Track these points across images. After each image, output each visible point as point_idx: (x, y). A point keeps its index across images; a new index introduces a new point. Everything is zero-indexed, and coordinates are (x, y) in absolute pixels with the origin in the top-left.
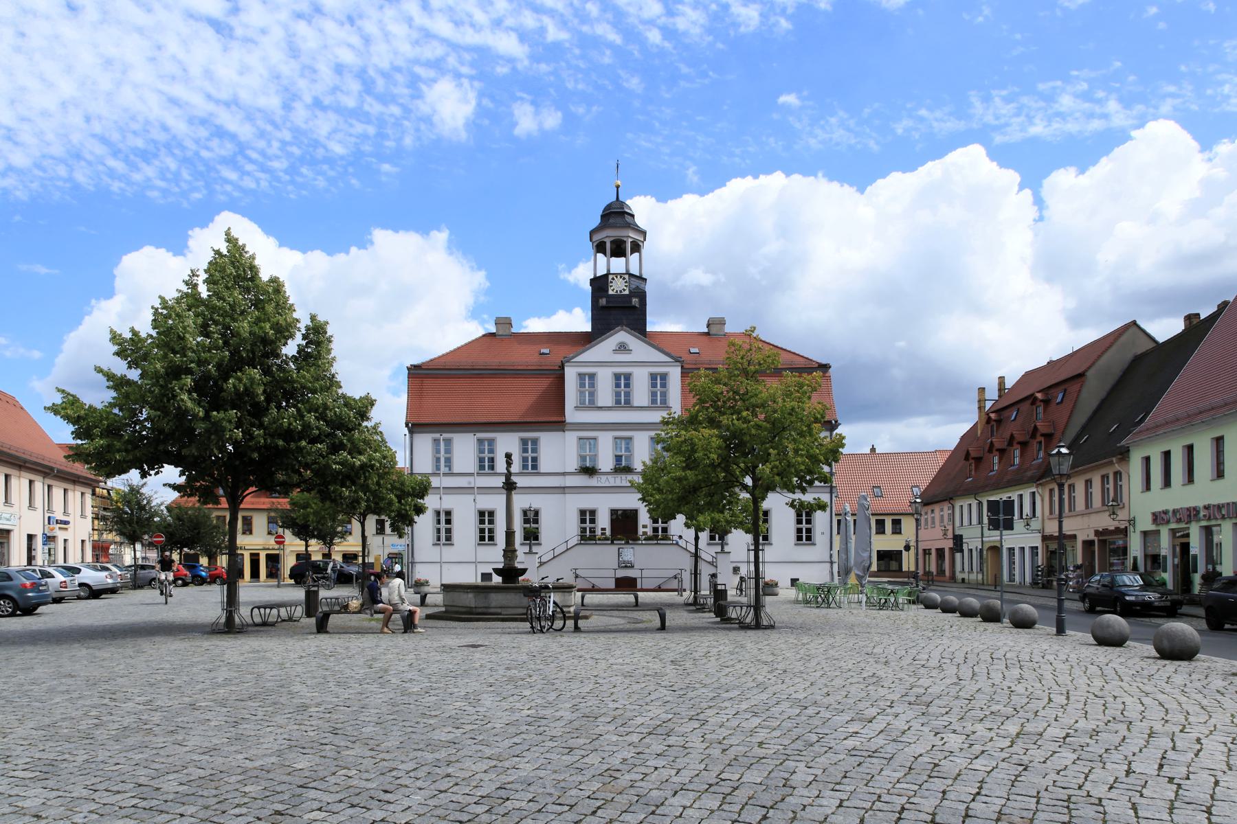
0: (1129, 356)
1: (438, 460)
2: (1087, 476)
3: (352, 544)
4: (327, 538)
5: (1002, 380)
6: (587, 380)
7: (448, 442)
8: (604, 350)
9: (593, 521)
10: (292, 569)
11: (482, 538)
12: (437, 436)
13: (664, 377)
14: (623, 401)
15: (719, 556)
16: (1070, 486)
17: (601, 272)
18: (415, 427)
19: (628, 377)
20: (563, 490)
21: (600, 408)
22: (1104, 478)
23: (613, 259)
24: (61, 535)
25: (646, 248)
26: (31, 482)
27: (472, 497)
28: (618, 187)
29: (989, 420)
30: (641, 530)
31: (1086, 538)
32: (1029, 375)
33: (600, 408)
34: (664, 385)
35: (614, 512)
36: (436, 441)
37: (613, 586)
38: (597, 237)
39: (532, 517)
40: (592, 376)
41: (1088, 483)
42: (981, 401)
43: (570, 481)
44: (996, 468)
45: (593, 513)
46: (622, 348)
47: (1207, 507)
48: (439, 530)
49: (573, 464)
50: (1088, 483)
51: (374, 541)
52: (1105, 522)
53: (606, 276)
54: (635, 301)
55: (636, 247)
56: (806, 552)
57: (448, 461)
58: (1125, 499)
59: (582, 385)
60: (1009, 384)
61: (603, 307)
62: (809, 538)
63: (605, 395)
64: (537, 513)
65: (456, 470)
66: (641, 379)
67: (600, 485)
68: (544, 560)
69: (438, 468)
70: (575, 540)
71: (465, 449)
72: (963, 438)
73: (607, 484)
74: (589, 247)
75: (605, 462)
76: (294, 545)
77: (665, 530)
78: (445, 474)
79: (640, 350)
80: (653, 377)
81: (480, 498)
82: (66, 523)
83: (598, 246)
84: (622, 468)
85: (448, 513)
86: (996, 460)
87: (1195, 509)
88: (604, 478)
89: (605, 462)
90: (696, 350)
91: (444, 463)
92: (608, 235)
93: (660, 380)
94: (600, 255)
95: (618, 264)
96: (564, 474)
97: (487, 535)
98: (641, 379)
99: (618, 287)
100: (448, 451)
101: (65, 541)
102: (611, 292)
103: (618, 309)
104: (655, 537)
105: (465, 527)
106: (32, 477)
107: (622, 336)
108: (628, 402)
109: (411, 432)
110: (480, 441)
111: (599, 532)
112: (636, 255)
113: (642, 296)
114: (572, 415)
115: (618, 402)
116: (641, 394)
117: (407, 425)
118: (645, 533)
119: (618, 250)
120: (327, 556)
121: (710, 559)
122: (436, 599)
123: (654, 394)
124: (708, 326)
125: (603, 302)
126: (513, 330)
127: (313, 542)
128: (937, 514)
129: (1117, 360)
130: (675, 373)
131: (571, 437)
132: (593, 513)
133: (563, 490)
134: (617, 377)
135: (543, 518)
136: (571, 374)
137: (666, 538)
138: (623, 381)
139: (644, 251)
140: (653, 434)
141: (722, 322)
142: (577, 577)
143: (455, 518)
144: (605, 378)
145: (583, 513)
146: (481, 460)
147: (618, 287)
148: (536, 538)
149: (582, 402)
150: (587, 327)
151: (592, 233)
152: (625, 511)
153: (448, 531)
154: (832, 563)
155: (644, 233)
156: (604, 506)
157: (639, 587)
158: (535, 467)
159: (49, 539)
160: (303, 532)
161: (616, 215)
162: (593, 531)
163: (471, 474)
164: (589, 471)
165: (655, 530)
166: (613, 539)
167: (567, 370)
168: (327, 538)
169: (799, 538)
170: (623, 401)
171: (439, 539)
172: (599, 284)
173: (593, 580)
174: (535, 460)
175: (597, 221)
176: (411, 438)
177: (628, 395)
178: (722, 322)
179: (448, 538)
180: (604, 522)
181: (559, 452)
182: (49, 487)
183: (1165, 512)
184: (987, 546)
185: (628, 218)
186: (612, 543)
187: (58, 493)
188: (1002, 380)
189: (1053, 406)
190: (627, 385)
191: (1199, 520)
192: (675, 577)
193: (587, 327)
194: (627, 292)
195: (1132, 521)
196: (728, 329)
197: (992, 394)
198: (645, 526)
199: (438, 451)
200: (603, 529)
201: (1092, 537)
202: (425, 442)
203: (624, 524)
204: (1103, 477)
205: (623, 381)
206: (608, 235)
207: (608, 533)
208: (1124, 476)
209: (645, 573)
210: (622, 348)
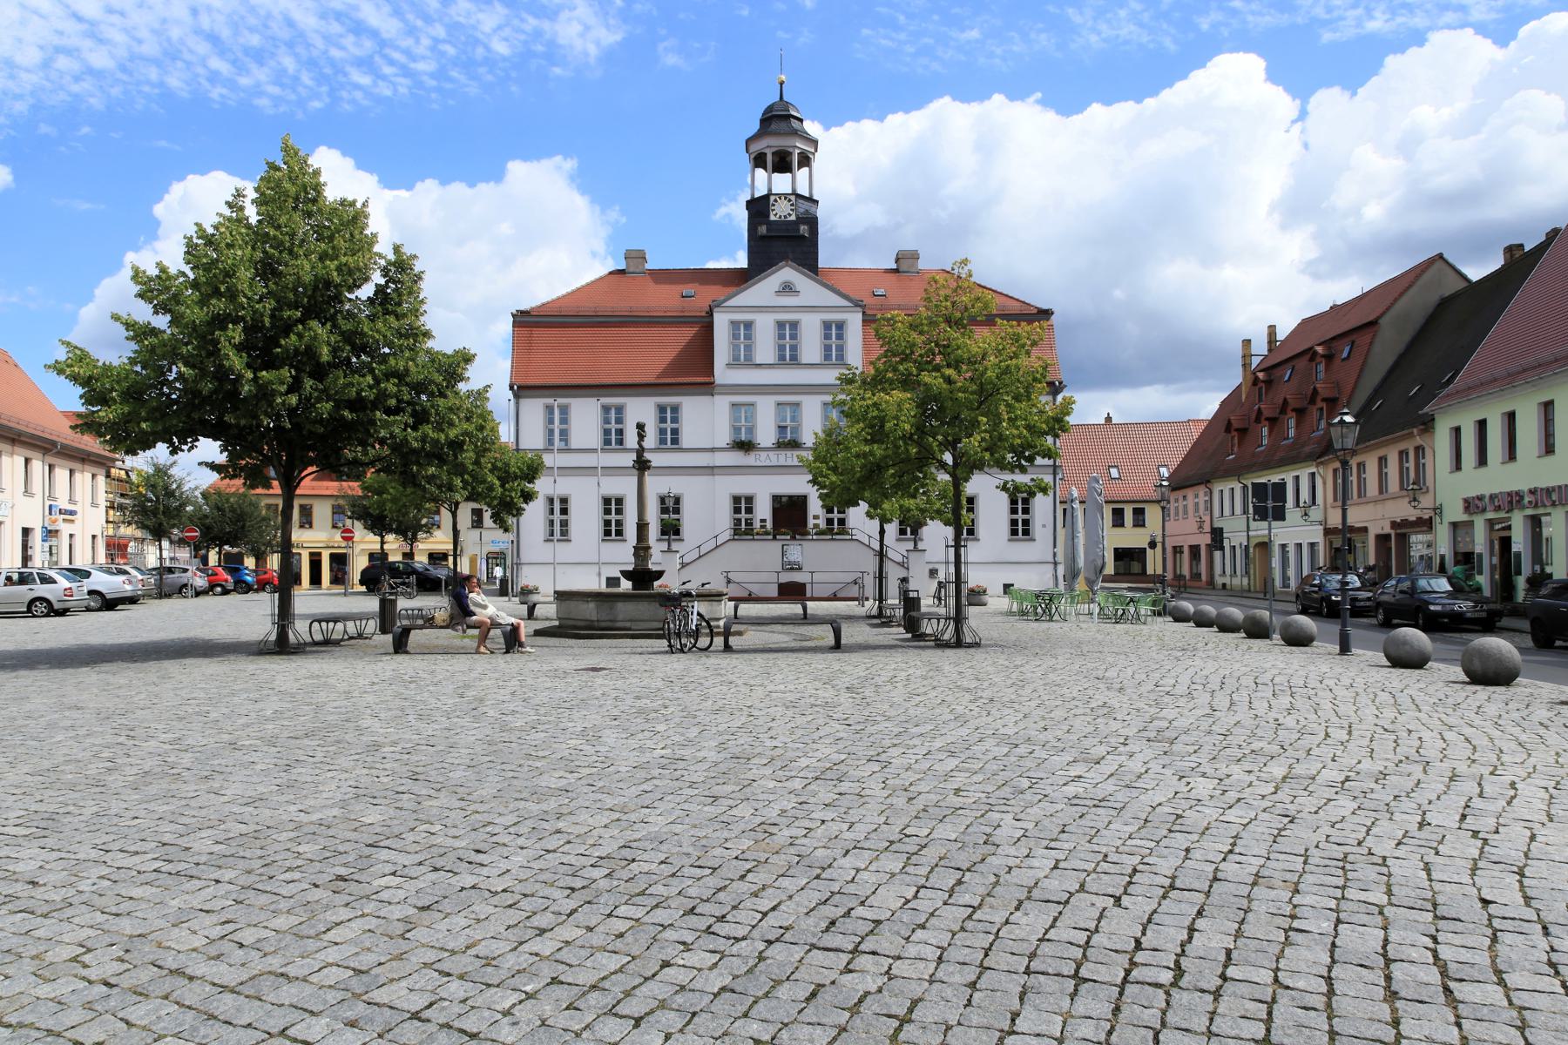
0: (1433, 298)
1: (551, 432)
2: (1381, 452)
3: (440, 540)
4: (409, 531)
5: (1272, 330)
7: (564, 410)
8: (764, 291)
9: (749, 510)
10: (364, 573)
11: (607, 533)
12: (550, 401)
13: (840, 326)
14: (789, 357)
15: (913, 556)
16: (1359, 465)
17: (761, 191)
18: (521, 390)
19: (794, 325)
20: (711, 470)
22: (1403, 455)
23: (776, 176)
24: (65, 529)
25: (818, 161)
26: (27, 461)
27: (594, 480)
28: (782, 83)
29: (1256, 381)
30: (811, 522)
31: (1380, 532)
32: (1306, 323)
34: (840, 337)
35: (776, 499)
36: (549, 409)
37: (775, 594)
38: (757, 147)
39: (671, 505)
40: (749, 325)
41: (1382, 461)
42: (1247, 356)
43: (719, 459)
44: (1265, 442)
45: (749, 499)
46: (787, 289)
47: (1532, 492)
49: (724, 437)
50: (1382, 461)
51: (469, 537)
52: (1403, 510)
53: (766, 198)
54: (804, 229)
55: (805, 160)
56: (1022, 550)
57: (564, 434)
58: (1429, 482)
59: (736, 336)
60: (1281, 335)
61: (763, 237)
62: (1026, 532)
63: (765, 349)
64: (677, 500)
66: (811, 327)
68: (686, 560)
69: (551, 442)
70: (727, 535)
71: (586, 417)
74: (745, 161)
75: (766, 435)
76: (366, 542)
77: (842, 522)
79: (809, 291)
80: (827, 325)
81: (605, 481)
82: (72, 513)
83: (756, 159)
84: (789, 443)
85: (564, 501)
86: (1265, 431)
87: (1517, 493)
88: (763, 454)
89: (766, 435)
91: (559, 435)
92: (769, 145)
93: (833, 330)
94: (760, 172)
95: (782, 183)
96: (713, 450)
97: (613, 528)
98: (811, 327)
100: (564, 421)
101: (71, 536)
102: (772, 218)
103: (783, 239)
104: (830, 531)
105: (586, 519)
106: (29, 453)
107: (787, 273)
108: (794, 358)
109: (517, 396)
110: (606, 409)
111: (757, 525)
112: (806, 170)
113: (812, 222)
114: (722, 373)
115: (782, 357)
116: (811, 348)
117: (511, 388)
118: (816, 526)
119: (782, 164)
120: (409, 555)
121: (900, 559)
122: (548, 611)
123: (828, 348)
124: (897, 261)
125: (763, 230)
126: (648, 266)
127: (390, 537)
129: (1420, 302)
130: (854, 321)
131: (721, 405)
132: (749, 499)
133: (711, 470)
134: (781, 325)
135: (686, 506)
136: (721, 321)
137: (843, 532)
138: (788, 330)
139: (815, 165)
140: (829, 398)
141: (914, 256)
142: (729, 582)
143: (573, 507)
144: (765, 326)
145: (736, 499)
146: (607, 432)
148: (677, 532)
149: (736, 358)
150: (742, 261)
151: (748, 142)
152: (790, 497)
153: (564, 524)
154: (1055, 564)
155: (815, 143)
156: (764, 491)
157: (808, 594)
158: (675, 441)
159: (50, 533)
160: (378, 524)
161: (777, 119)
162: (749, 523)
163: (594, 450)
164: (745, 446)
165: (830, 522)
166: (776, 533)
167: (716, 316)
168: (409, 531)
169: (1014, 532)
170: (789, 357)
172: (758, 207)
174: (675, 432)
176: (517, 404)
177: (794, 348)
178: (914, 256)
179: (564, 533)
180: (763, 511)
181: (705, 421)
182: (51, 467)
183: (1480, 498)
184: (1253, 542)
185: (795, 124)
186: (774, 538)
187: (61, 474)
188: (1272, 330)
189: (1337, 362)
190: (793, 337)
191: (1523, 508)
193: (742, 261)
194: (793, 218)
195: (1438, 510)
196: (922, 265)
197: (1260, 347)
198: (816, 517)
199: (551, 421)
200: (763, 521)
201: (1388, 530)
202: (534, 409)
203: (790, 515)
204: (1401, 453)
205: (788, 330)
207: (769, 525)
208: (1428, 452)
210: (787, 289)
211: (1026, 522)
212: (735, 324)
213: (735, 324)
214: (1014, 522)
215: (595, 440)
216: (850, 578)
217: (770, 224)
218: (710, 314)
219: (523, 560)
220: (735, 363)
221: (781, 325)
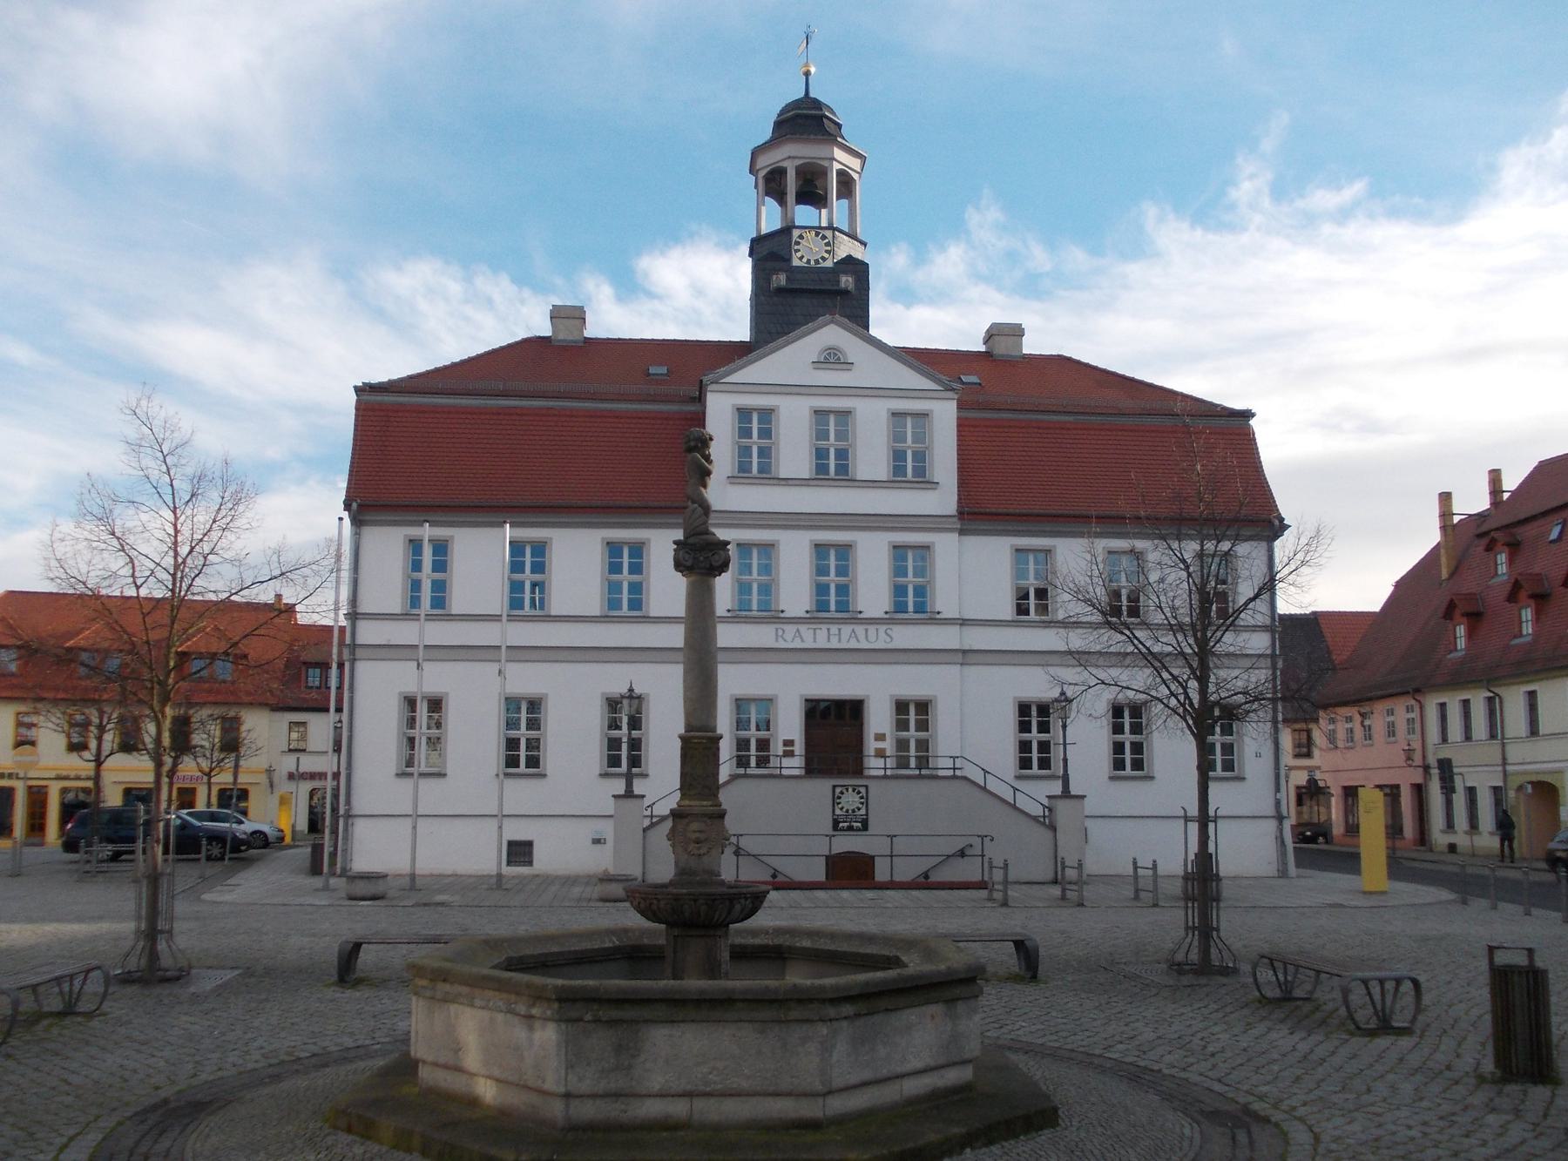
1: (416, 586)
5: (1495, 477)
6: (756, 424)
7: (441, 548)
8: (795, 360)
11: (512, 762)
14: (833, 465)
15: (1063, 807)
21: (787, 482)
27: (495, 667)
30: (871, 745)
33: (787, 482)
36: (415, 545)
37: (820, 876)
40: (767, 414)
46: (832, 359)
48: (416, 586)
54: (847, 281)
57: (440, 587)
60: (1510, 483)
61: (780, 291)
65: (457, 605)
66: (871, 421)
69: (415, 601)
71: (480, 556)
72: (1399, 585)
73: (798, 644)
78: (429, 618)
81: (513, 669)
85: (436, 704)
88: (790, 630)
90: (973, 379)
91: (430, 593)
92: (792, 155)
95: (805, 215)
97: (523, 753)
98: (871, 421)
99: (807, 252)
100: (440, 566)
102: (796, 262)
107: (831, 334)
108: (843, 469)
109: (357, 522)
111: (777, 748)
115: (821, 469)
121: (1037, 810)
125: (781, 280)
128: (1378, 722)
141: (1017, 332)
143: (453, 715)
147: (807, 252)
149: (744, 467)
150: (741, 331)
151: (755, 153)
154: (1280, 818)
158: (636, 604)
163: (495, 618)
169: (1119, 765)
170: (833, 465)
173: (776, 863)
174: (636, 588)
175: (767, 134)
180: (790, 726)
184: (1514, 783)
188: (1495, 477)
192: (962, 854)
193: (741, 331)
194: (829, 264)
198: (880, 737)
199: (417, 566)
202: (388, 545)
206: (792, 155)
209: (901, 846)
212: (744, 414)
213: (744, 414)
215: (494, 598)
217: (792, 271)
218: (700, 399)
219: (355, 811)
220: (742, 473)
221: (821, 414)
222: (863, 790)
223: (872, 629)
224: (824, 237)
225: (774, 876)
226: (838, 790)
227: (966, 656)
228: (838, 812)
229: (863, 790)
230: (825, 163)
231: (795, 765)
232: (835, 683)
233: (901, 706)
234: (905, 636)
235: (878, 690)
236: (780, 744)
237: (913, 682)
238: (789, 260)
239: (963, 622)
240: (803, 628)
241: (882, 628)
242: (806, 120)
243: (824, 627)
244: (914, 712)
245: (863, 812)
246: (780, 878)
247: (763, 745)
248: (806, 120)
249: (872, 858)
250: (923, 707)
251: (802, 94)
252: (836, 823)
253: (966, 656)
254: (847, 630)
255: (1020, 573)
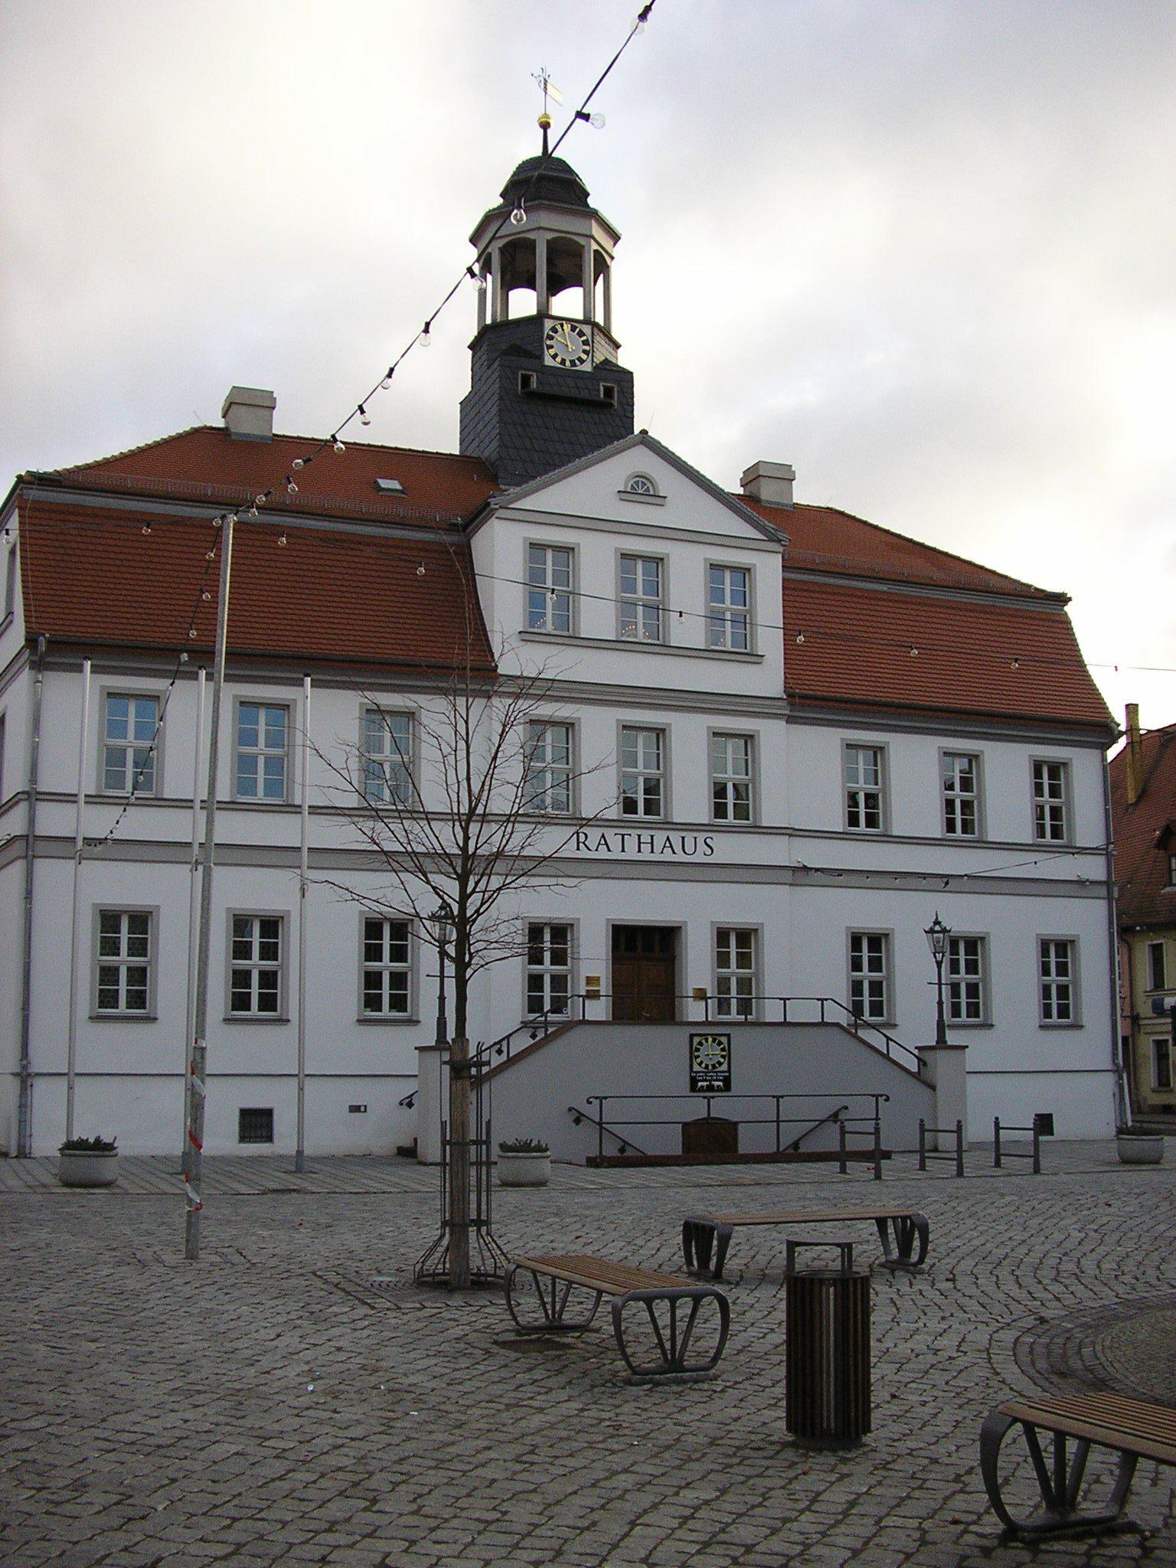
14: (646, 623)
37: (674, 1145)
40: (567, 551)
67: (584, 853)
88: (594, 835)
92: (540, 225)
102: (548, 361)
130: (769, 573)
132: (561, 932)
156: (595, 910)
170: (646, 623)
171: (1047, 1014)
180: (593, 957)
194: (587, 367)
200: (590, 980)
206: (540, 225)
211: (269, 979)
214: (372, 980)
216: (824, 1108)
222: (724, 1040)
223: (689, 837)
224: (581, 334)
225: (622, 1150)
226: (696, 1040)
227: (801, 875)
228: (696, 1068)
229: (724, 1040)
230: (582, 241)
231: (599, 1010)
232: (648, 904)
233: (722, 936)
234: (731, 848)
235: (696, 912)
236: (583, 982)
237: (736, 905)
238: (541, 357)
239: (792, 833)
240: (610, 834)
241: (701, 837)
242: (546, 184)
243: (634, 832)
244: (738, 942)
245: (724, 1067)
246: (629, 1152)
247: (559, 982)
248: (546, 184)
249: (736, 1124)
250: (745, 936)
251: (539, 152)
252: (694, 1082)
253: (801, 875)
254: (660, 837)
255: (850, 774)
